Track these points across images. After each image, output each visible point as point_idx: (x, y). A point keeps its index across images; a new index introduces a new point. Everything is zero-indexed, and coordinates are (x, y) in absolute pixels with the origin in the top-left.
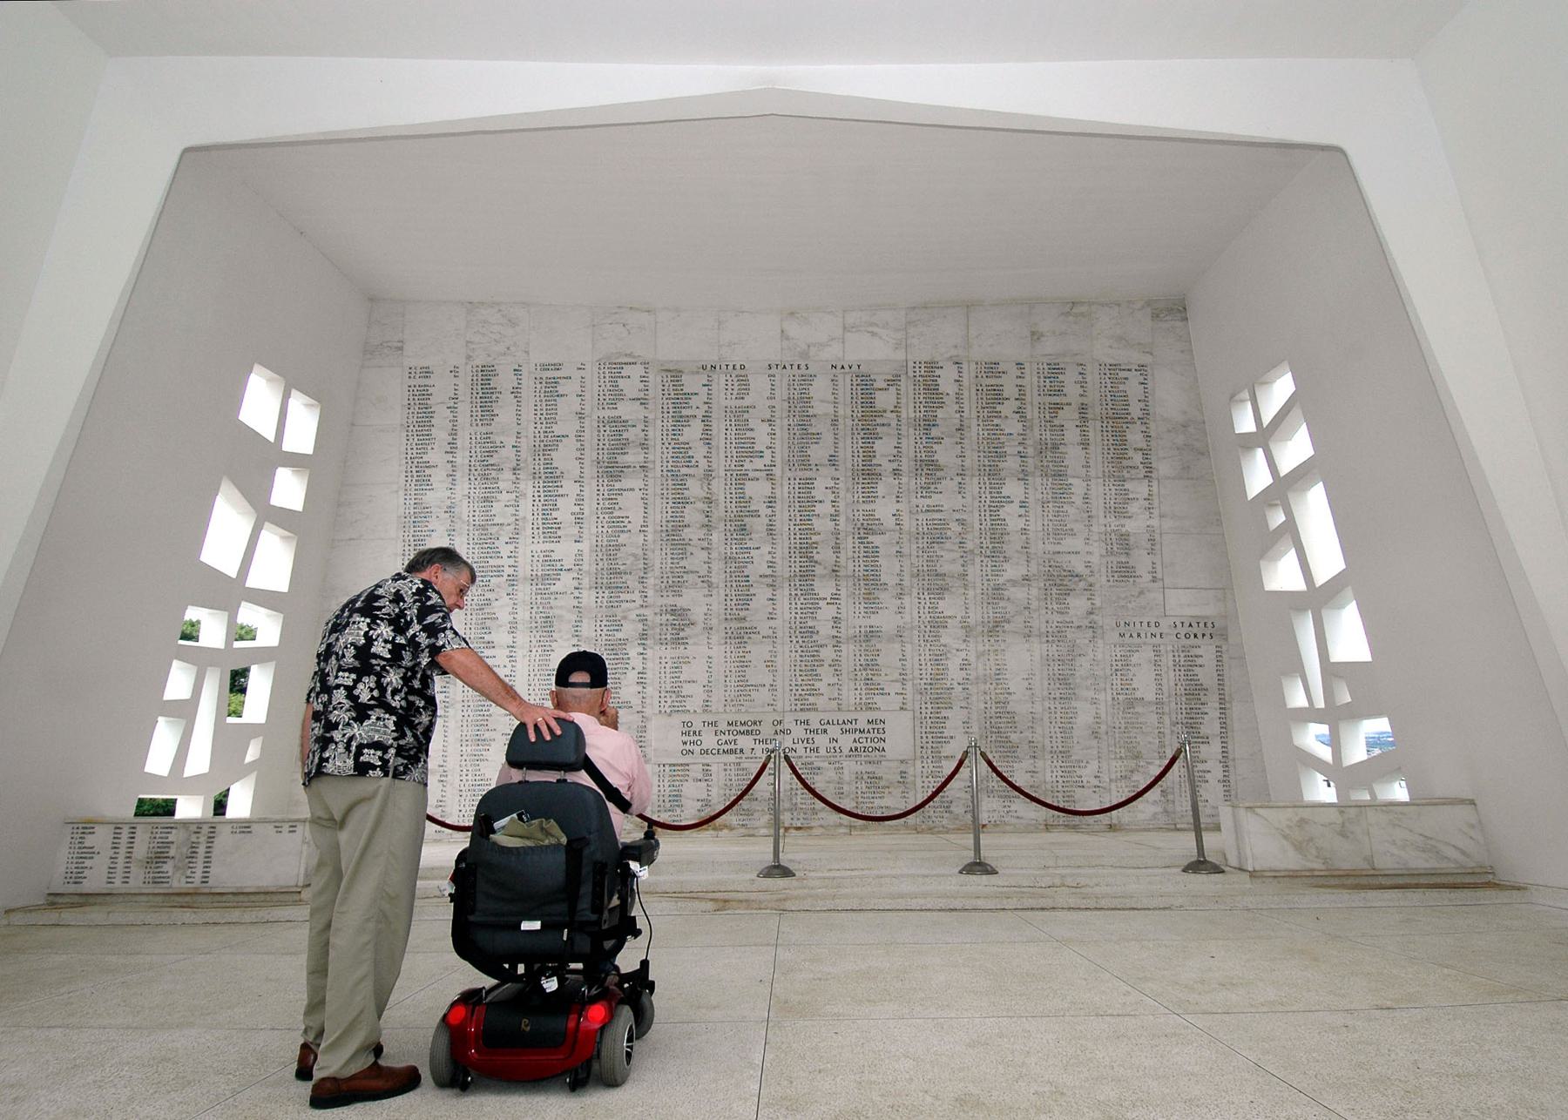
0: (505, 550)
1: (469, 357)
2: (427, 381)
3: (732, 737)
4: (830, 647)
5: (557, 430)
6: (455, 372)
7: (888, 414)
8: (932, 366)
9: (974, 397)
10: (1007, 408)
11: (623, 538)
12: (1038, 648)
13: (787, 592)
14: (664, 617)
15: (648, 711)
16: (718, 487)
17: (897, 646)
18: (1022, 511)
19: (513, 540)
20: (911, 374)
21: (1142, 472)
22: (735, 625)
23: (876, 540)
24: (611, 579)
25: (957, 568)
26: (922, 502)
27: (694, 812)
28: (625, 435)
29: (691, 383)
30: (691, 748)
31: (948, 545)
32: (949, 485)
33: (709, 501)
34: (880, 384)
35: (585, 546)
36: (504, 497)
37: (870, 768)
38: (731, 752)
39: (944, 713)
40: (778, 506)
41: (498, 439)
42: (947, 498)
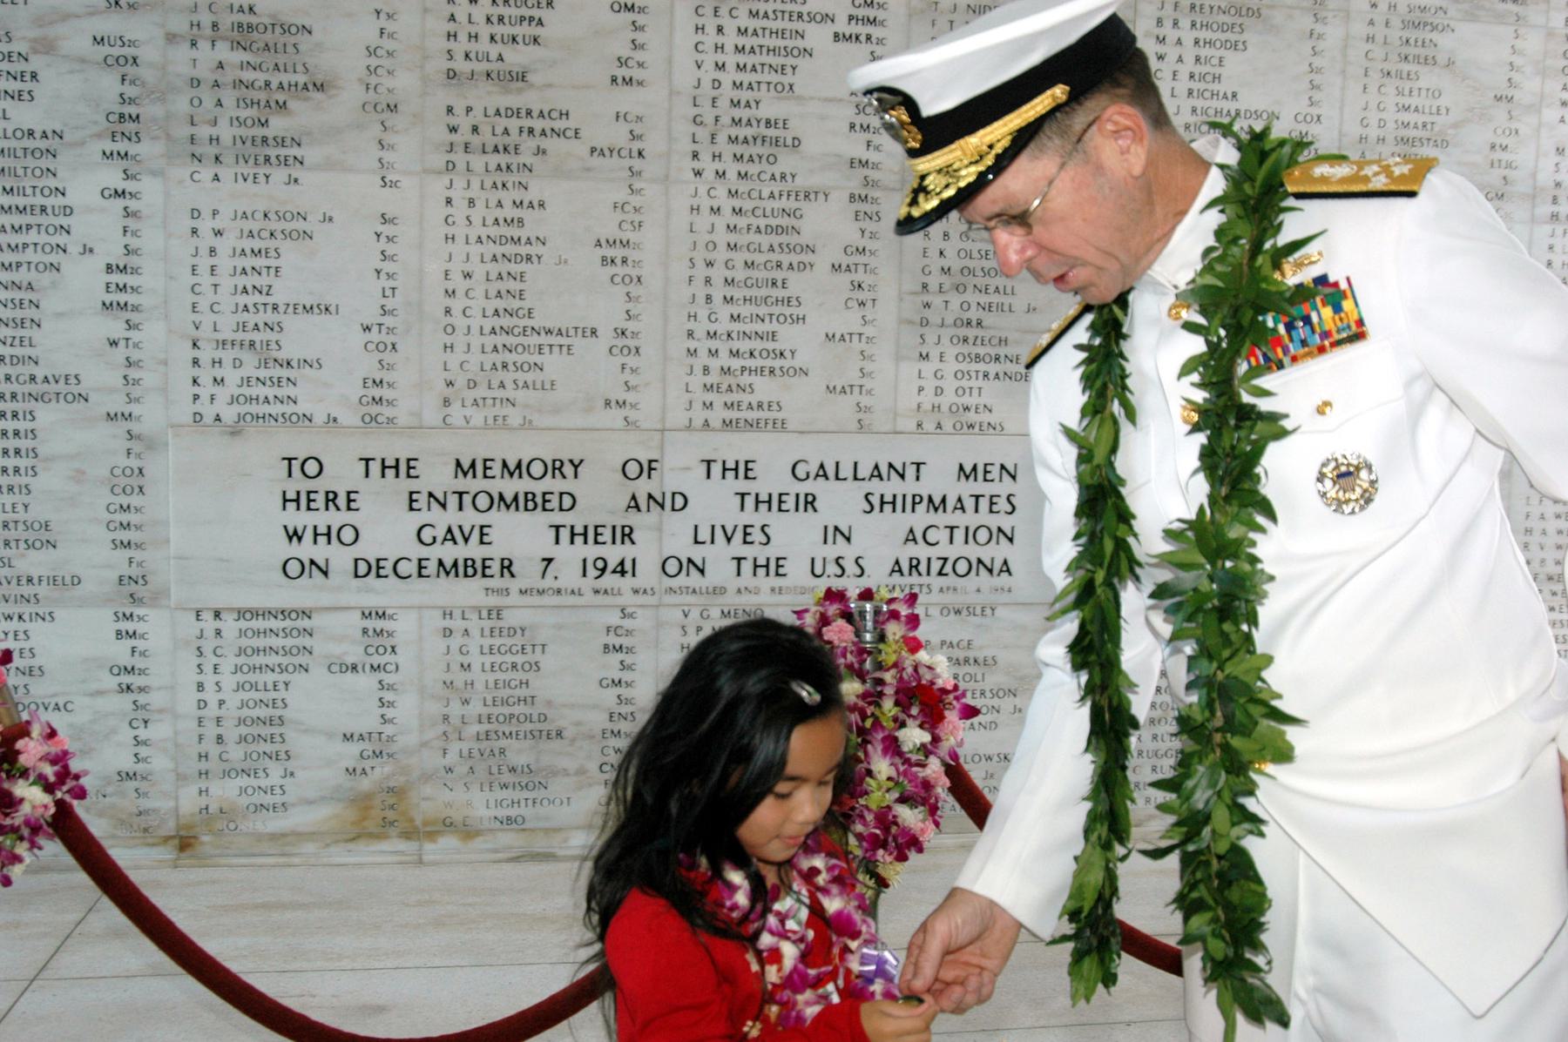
3: (470, 518)
4: (839, 199)
14: (207, 54)
15: (151, 416)
22: (487, 97)
27: (333, 776)
30: (321, 552)
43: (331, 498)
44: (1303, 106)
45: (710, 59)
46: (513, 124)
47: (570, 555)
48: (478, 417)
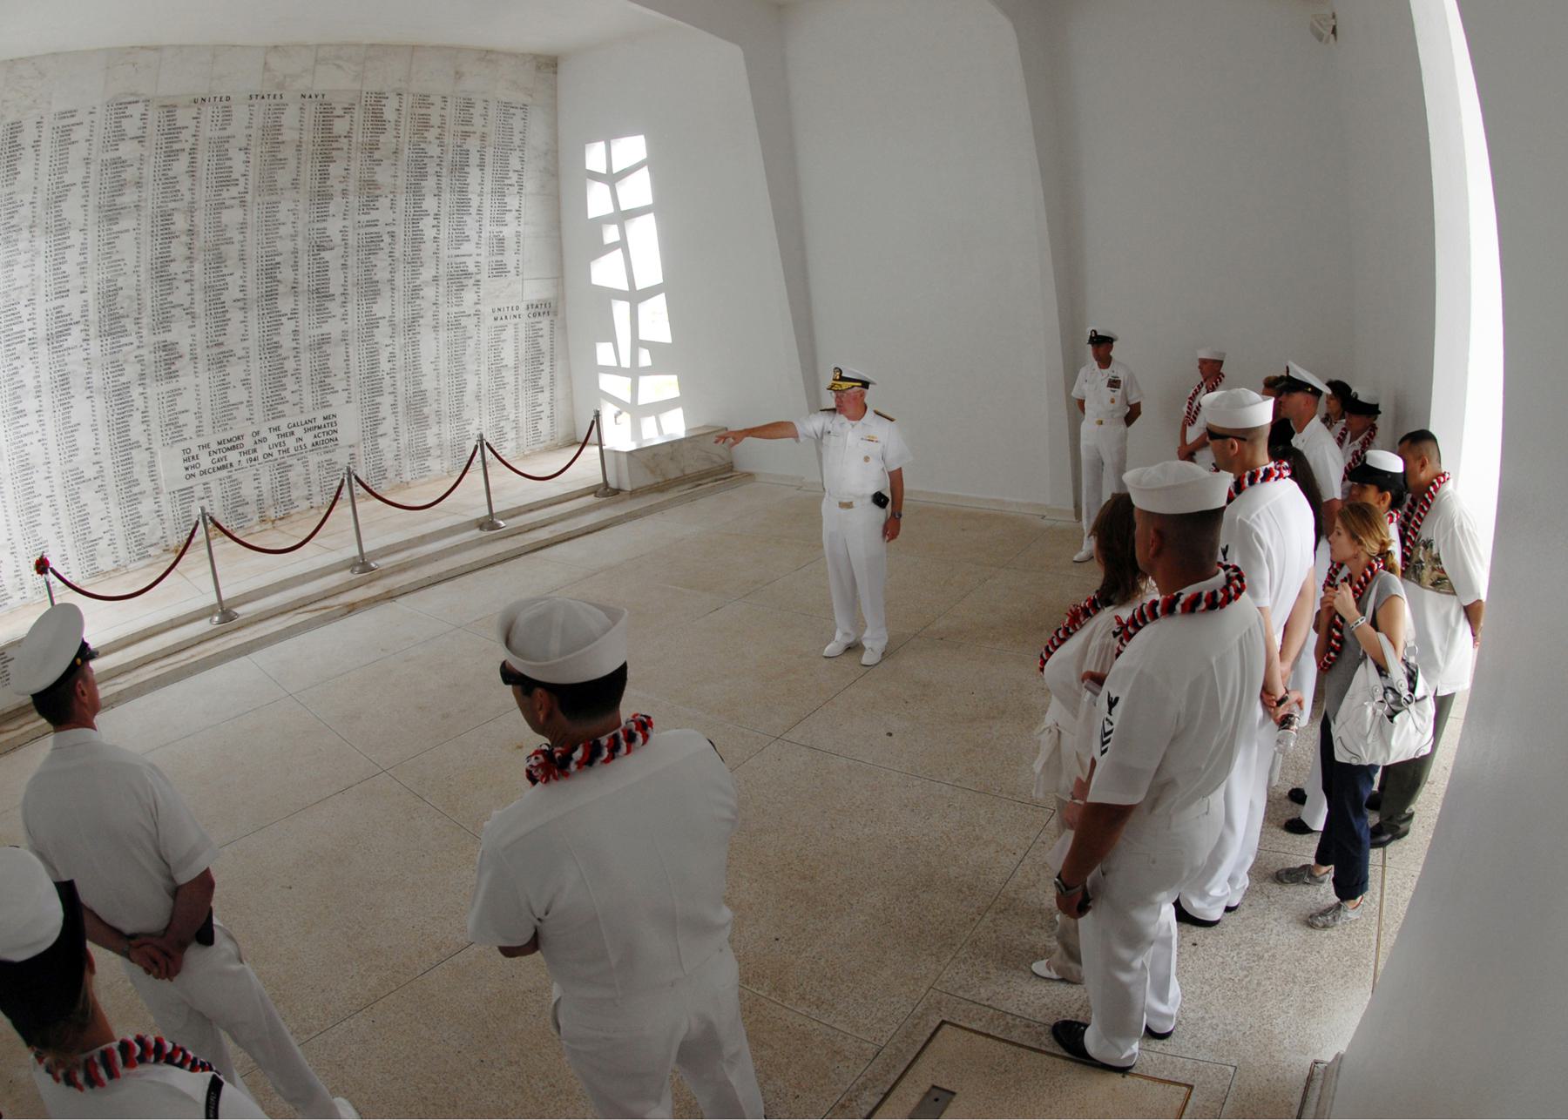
10: (431, 135)
12: (443, 335)
17: (343, 349)
23: (326, 255)
32: (384, 202)
37: (328, 456)
38: (224, 467)
39: (378, 400)
42: (382, 214)
47: (244, 458)
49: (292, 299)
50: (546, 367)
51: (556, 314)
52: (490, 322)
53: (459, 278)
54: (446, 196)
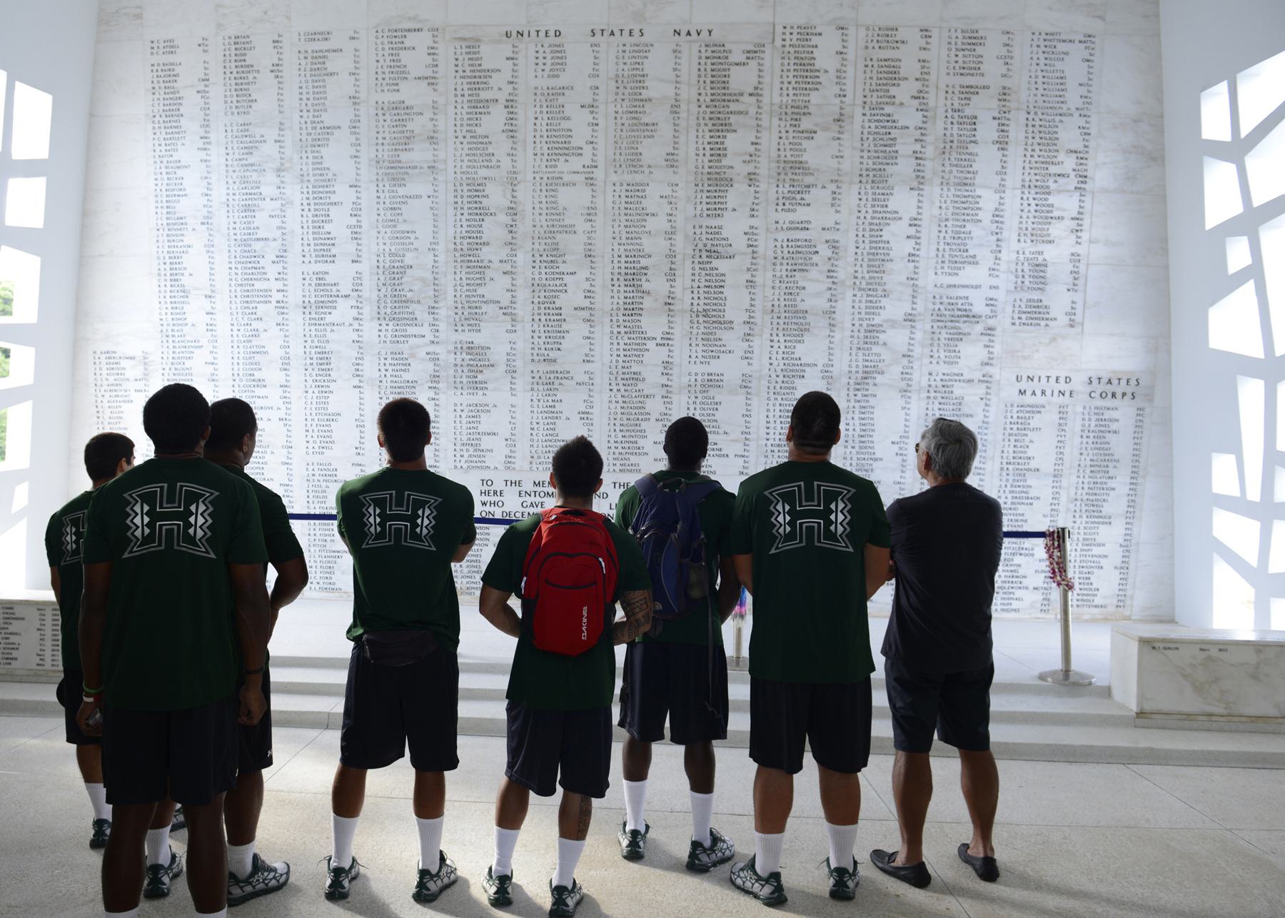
0: (272, 271)
1: (219, 26)
2: (171, 59)
3: (538, 499)
4: (658, 398)
5: (328, 119)
6: (203, 45)
7: (746, 99)
8: (807, 33)
9: (861, 76)
10: (903, 92)
11: (409, 259)
13: (608, 330)
14: (459, 356)
16: (525, 194)
17: (741, 399)
18: (912, 231)
19: (281, 257)
20: (778, 43)
21: (1072, 182)
22: (545, 367)
23: (722, 265)
24: (396, 304)
25: (823, 304)
26: (786, 217)
28: (410, 126)
29: (493, 56)
31: (813, 273)
33: (512, 211)
34: (737, 56)
35: (365, 267)
36: (268, 206)
40: (599, 219)
41: (257, 131)
42: (817, 212)
43: (495, 493)
44: (826, 361)
45: (615, 353)
46: (552, 376)
48: (541, 467)
49: (665, 319)
50: (1121, 483)
51: (1150, 398)
52: (1010, 393)
53: (955, 320)
54: (933, 191)
